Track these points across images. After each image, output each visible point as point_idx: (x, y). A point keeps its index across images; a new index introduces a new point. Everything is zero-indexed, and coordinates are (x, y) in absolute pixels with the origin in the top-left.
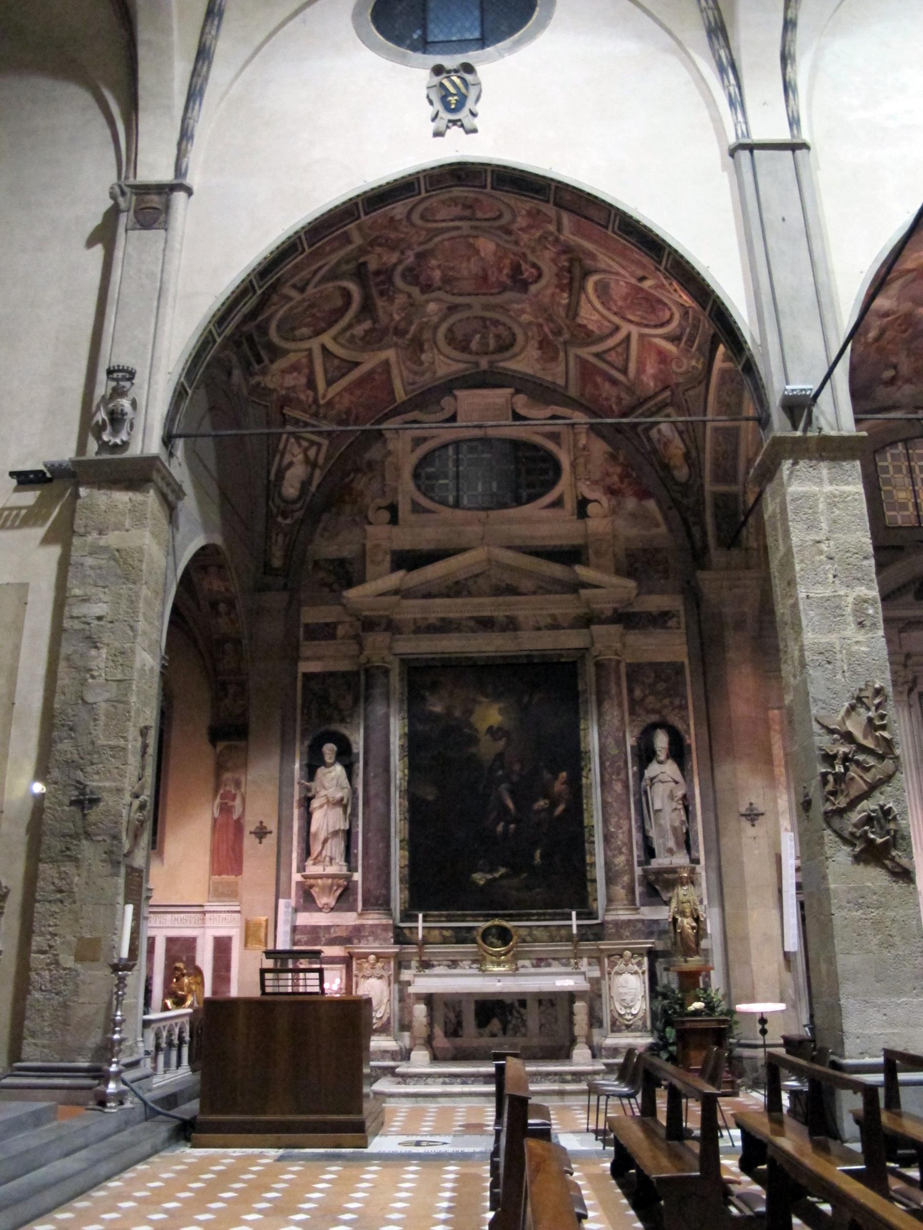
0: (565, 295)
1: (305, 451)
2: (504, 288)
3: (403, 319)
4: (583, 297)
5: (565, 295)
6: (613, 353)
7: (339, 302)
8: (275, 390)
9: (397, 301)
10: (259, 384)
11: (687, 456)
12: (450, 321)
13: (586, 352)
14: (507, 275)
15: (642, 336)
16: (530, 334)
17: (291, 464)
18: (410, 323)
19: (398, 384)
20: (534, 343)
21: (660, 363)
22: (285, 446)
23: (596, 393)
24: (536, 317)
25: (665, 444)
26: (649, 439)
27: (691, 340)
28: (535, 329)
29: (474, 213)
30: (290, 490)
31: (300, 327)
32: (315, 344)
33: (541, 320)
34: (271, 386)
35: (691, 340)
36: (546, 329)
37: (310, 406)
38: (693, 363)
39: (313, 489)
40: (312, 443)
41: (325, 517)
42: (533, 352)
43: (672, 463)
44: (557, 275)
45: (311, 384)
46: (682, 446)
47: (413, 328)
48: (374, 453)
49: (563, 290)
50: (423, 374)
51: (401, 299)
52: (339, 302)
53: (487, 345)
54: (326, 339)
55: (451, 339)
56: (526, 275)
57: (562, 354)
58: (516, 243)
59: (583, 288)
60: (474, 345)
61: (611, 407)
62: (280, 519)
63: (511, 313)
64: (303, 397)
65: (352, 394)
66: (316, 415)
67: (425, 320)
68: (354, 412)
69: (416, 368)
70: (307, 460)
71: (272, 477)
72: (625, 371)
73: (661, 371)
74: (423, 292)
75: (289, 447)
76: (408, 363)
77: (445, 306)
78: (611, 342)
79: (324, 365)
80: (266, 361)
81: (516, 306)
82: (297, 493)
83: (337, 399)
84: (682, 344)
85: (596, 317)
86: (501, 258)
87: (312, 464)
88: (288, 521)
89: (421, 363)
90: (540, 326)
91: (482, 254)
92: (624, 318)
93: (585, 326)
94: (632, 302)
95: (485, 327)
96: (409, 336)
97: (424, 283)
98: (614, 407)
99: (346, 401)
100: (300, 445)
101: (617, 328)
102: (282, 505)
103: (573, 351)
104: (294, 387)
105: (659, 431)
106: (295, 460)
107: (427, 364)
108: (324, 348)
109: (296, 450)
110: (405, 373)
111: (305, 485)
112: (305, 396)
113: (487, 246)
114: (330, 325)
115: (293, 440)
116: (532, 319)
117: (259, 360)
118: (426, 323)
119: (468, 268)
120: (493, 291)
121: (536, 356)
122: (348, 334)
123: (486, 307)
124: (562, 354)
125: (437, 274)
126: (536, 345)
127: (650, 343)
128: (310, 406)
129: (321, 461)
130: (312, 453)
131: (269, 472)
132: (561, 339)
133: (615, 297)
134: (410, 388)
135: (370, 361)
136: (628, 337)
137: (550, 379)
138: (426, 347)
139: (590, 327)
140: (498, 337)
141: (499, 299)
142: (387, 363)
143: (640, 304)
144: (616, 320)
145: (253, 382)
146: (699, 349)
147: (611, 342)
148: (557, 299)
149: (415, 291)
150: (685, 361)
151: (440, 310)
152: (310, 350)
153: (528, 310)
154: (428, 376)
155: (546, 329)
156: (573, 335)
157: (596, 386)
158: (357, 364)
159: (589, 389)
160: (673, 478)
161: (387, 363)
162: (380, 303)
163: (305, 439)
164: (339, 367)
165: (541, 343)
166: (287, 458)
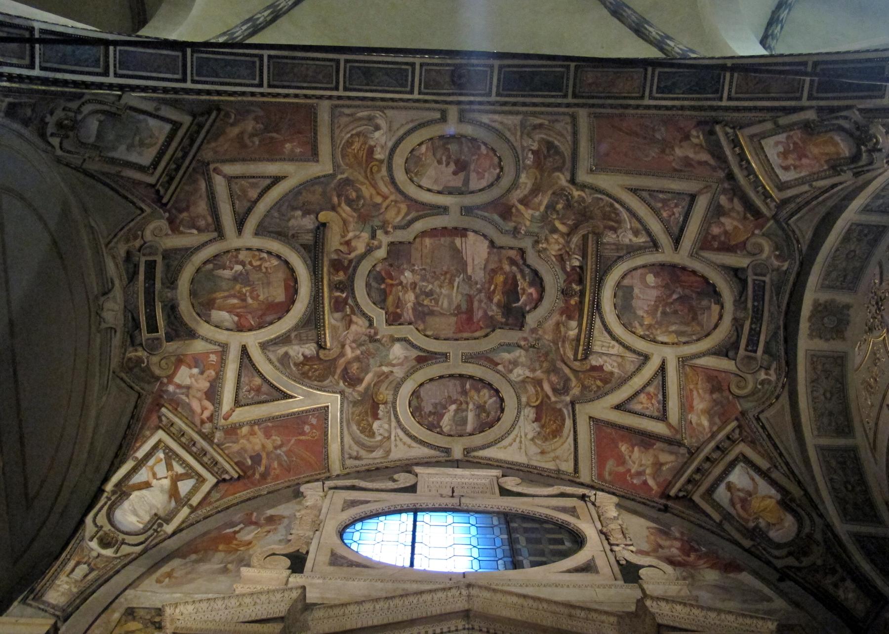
0: (574, 324)
1: (176, 479)
2: (493, 325)
3: (357, 359)
4: (598, 323)
5: (574, 324)
6: (642, 397)
7: (279, 295)
8: (158, 378)
9: (353, 328)
10: (139, 360)
11: (787, 503)
12: (422, 375)
13: (603, 409)
14: (498, 305)
15: (683, 361)
16: (524, 399)
17: (147, 485)
18: (365, 370)
19: (334, 449)
20: (530, 413)
21: (712, 392)
22: (148, 456)
23: (621, 469)
24: (533, 370)
25: (744, 501)
26: (717, 506)
27: (753, 342)
28: (531, 389)
29: (466, 181)
31: (220, 309)
32: (235, 341)
33: (539, 374)
34: (157, 371)
35: (753, 342)
36: (547, 387)
37: (203, 422)
38: (762, 376)
40: (191, 473)
41: (176, 563)
42: (528, 427)
43: (762, 524)
44: (564, 292)
45: (213, 394)
46: (773, 492)
47: (368, 378)
48: (282, 510)
49: (570, 318)
50: (371, 449)
51: (359, 326)
52: (279, 295)
53: (464, 422)
54: (252, 340)
55: (416, 411)
56: (523, 299)
57: (568, 423)
58: (515, 232)
59: (597, 306)
60: (446, 422)
61: (645, 483)
62: (94, 544)
63: (500, 367)
64: (196, 406)
65: (268, 435)
66: (208, 438)
67: (385, 369)
68: (264, 461)
69: (363, 438)
70: (174, 493)
72: (663, 417)
73: (716, 402)
74: (389, 323)
75: (151, 462)
76: (355, 428)
77: (415, 353)
78: (638, 382)
79: (239, 375)
80: (162, 333)
81: (506, 356)
82: (141, 526)
83: (245, 430)
84: (742, 352)
85: (617, 349)
86: (494, 272)
88: (109, 552)
89: (372, 434)
90: (538, 383)
91: (470, 271)
92: (654, 341)
93: (600, 368)
94: (664, 313)
95: (464, 393)
96: (361, 388)
97: (391, 309)
98: (651, 482)
99: (258, 442)
100: (169, 467)
101: (646, 358)
102: (107, 527)
103: (584, 411)
104: (188, 388)
105: (729, 487)
107: (379, 438)
108: (244, 350)
109: (161, 470)
110: (347, 439)
111: (158, 520)
112: (199, 406)
113: (476, 250)
114: (260, 327)
115: (161, 455)
116: (528, 373)
117: (153, 327)
118: (387, 376)
119: (450, 296)
120: (477, 334)
121: (530, 436)
122: (282, 351)
123: (467, 359)
124: (568, 423)
125: (410, 297)
126: (532, 415)
127: (693, 367)
128: (203, 422)
129: (195, 501)
132: (568, 399)
133: (640, 313)
134: (349, 463)
135: (302, 399)
136: (663, 368)
137: (551, 466)
139: (608, 368)
140: (481, 408)
141: (484, 345)
143: (675, 312)
144: (642, 345)
145: (131, 354)
146: (767, 351)
147: (638, 382)
148: (562, 329)
149: (378, 315)
150: (749, 377)
151: (406, 357)
152: (224, 348)
153: (523, 359)
154: (378, 454)
155: (547, 387)
156: (584, 388)
157: (621, 460)
158: (287, 396)
159: (610, 464)
160: (770, 540)
162: (331, 319)
163: (183, 462)
164: (258, 390)
165: (539, 409)
166: (143, 475)
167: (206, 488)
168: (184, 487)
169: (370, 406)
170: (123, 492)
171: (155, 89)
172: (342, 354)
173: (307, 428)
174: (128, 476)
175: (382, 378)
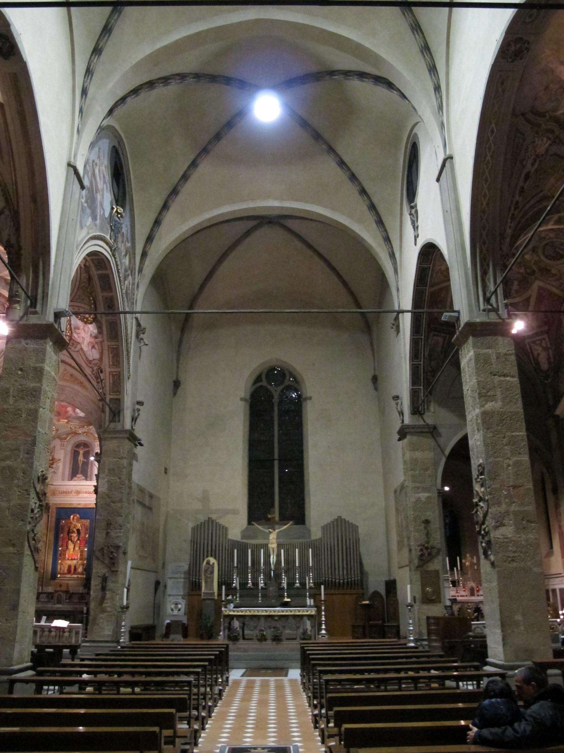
1: (540, 345)
3: (525, 269)
17: (539, 354)
30: (545, 366)
39: (552, 360)
40: (541, 340)
47: (534, 268)
55: (554, 258)
62: (546, 382)
67: (533, 262)
71: (534, 365)
76: (551, 279)
87: (545, 349)
88: (549, 380)
89: (555, 275)
100: (537, 345)
106: (539, 351)
110: (554, 283)
111: (548, 359)
129: (549, 346)
130: (544, 344)
131: (532, 363)
138: (549, 268)
142: (540, 288)
161: (540, 288)
166: (535, 353)
167: (547, 339)
168: (544, 344)
169: (545, 271)
170: (538, 363)
171: (424, 348)
172: (522, 274)
173: (544, 294)
174: (534, 358)
175: (536, 263)
